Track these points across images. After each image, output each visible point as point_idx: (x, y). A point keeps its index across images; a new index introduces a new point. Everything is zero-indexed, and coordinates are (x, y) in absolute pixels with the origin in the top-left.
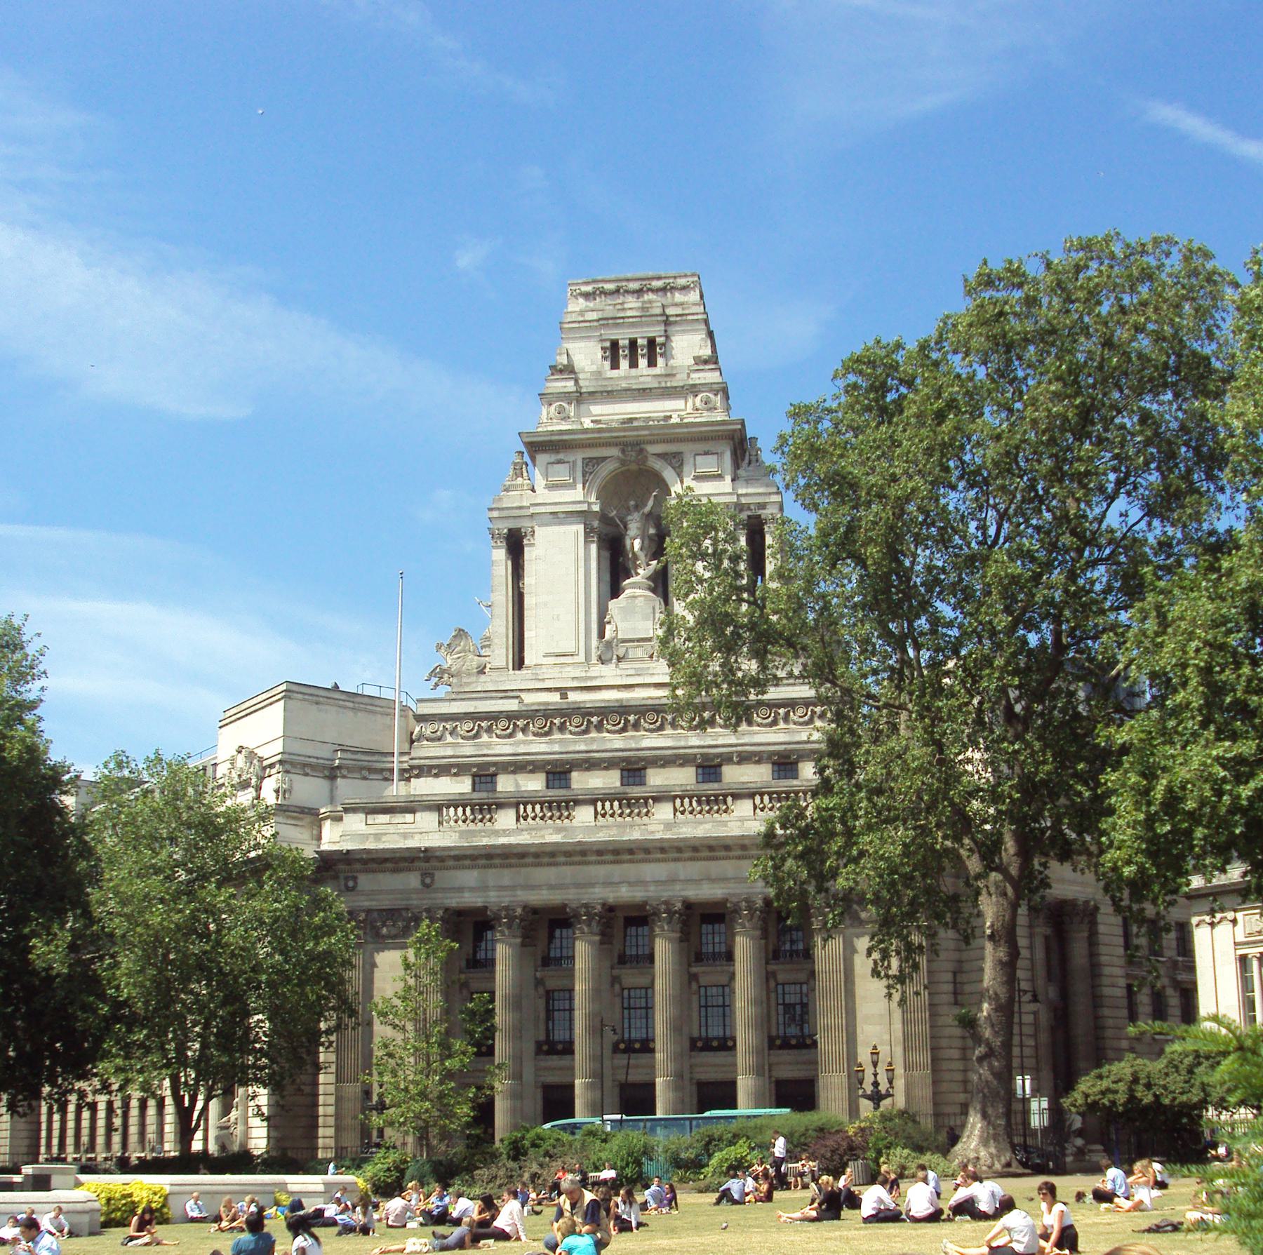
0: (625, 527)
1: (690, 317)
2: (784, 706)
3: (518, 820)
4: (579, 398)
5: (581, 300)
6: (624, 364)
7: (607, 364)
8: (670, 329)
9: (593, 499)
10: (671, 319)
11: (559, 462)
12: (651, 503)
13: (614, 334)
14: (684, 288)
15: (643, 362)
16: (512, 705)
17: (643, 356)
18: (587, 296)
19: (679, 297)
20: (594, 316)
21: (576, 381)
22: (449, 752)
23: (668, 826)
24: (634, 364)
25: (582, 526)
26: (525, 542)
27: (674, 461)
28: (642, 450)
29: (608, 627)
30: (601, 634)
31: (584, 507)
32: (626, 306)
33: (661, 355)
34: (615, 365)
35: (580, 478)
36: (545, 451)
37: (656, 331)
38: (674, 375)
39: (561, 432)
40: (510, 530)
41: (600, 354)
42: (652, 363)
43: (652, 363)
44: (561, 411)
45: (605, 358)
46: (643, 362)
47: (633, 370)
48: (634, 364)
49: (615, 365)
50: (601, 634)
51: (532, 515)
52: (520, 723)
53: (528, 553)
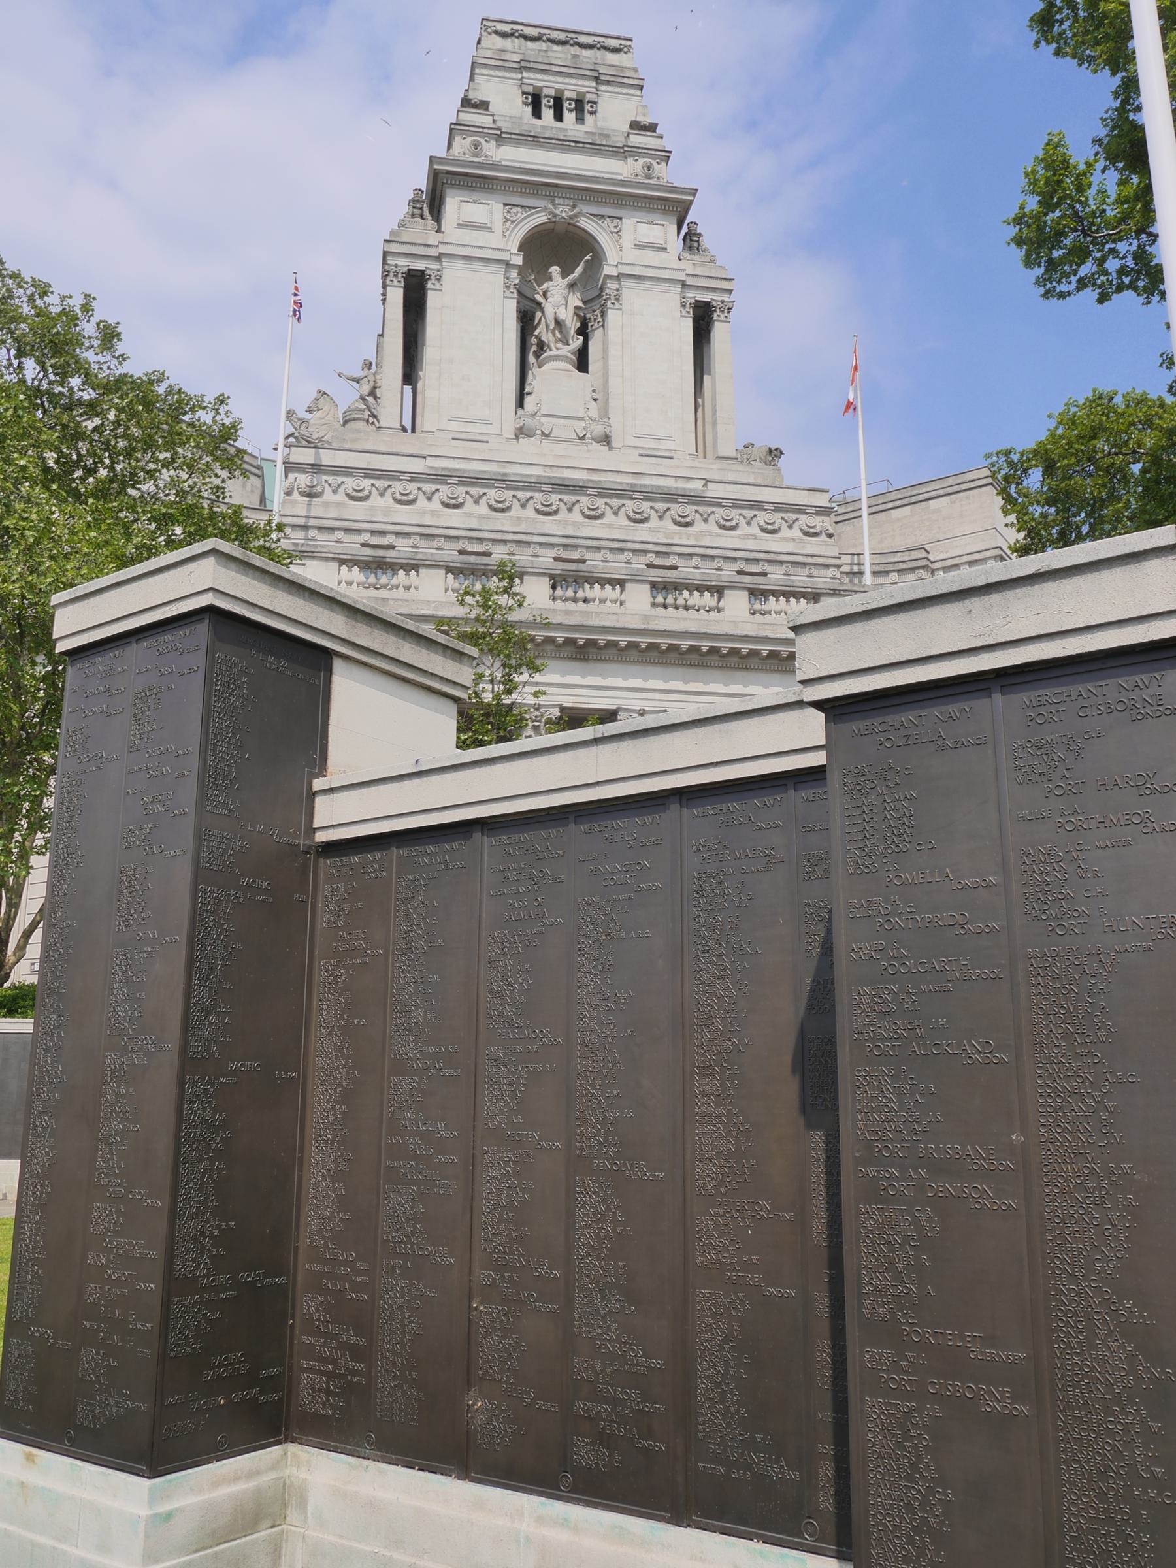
0: (545, 295)
1: (626, 81)
2: (751, 508)
3: (446, 590)
4: (500, 138)
5: (498, 39)
6: (548, 114)
7: (529, 109)
8: (602, 88)
9: (515, 250)
10: (602, 78)
11: (475, 202)
12: (579, 269)
13: (535, 80)
14: (617, 50)
15: (569, 117)
16: (417, 466)
17: (570, 110)
18: (504, 35)
19: (612, 58)
20: (516, 58)
21: (494, 121)
22: (333, 513)
23: (646, 617)
24: (559, 117)
25: (499, 280)
26: (429, 285)
27: (612, 226)
28: (574, 207)
29: (528, 400)
30: (520, 404)
31: (504, 256)
32: (550, 54)
33: (592, 113)
34: (537, 113)
35: (498, 226)
36: (460, 187)
37: (586, 87)
38: (607, 136)
39: (481, 166)
40: (409, 270)
41: (519, 99)
42: (580, 119)
43: (580, 119)
44: (476, 145)
45: (526, 104)
46: (569, 117)
47: (559, 124)
48: (559, 117)
49: (537, 113)
50: (520, 404)
51: (438, 258)
52: (429, 487)
53: (433, 300)
